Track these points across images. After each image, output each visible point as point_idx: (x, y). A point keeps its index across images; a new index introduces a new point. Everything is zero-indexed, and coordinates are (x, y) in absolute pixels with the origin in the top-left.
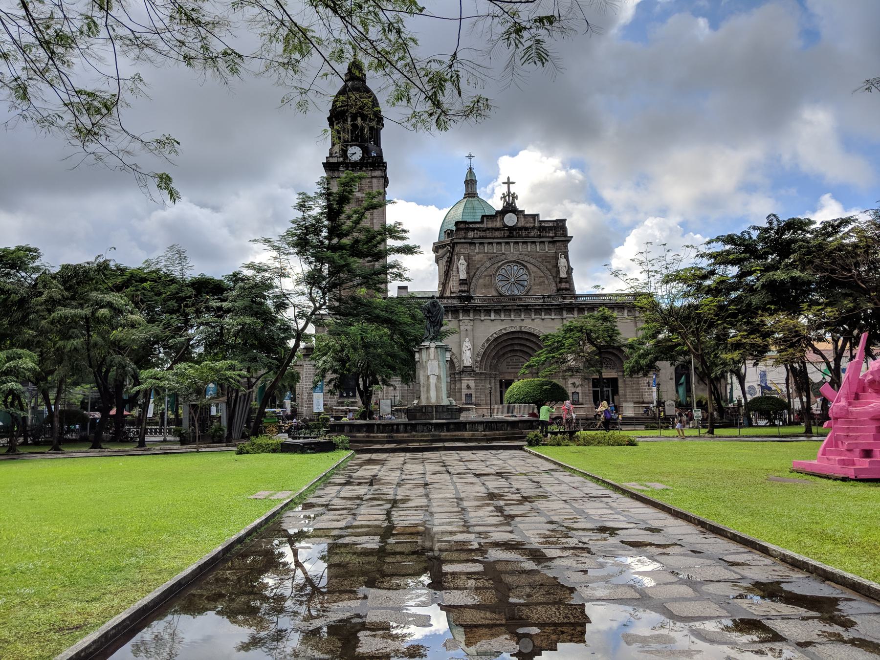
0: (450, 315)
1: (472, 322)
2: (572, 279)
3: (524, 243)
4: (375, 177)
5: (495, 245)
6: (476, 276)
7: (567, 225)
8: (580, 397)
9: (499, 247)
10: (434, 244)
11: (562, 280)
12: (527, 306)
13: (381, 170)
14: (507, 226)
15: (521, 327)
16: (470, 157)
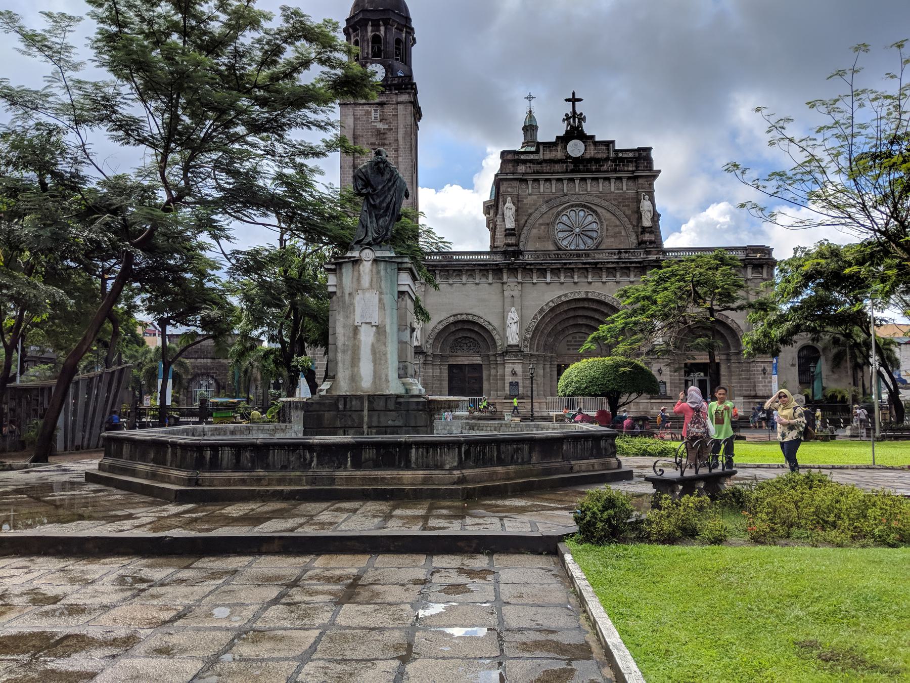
0: (490, 276)
1: (520, 287)
2: (659, 229)
3: (593, 179)
4: (401, 103)
5: (554, 182)
6: (527, 224)
7: (654, 154)
8: (668, 389)
9: (559, 185)
10: (485, 203)
11: (644, 230)
12: (597, 263)
13: (409, 93)
14: (570, 157)
15: (587, 293)
16: (530, 98)
